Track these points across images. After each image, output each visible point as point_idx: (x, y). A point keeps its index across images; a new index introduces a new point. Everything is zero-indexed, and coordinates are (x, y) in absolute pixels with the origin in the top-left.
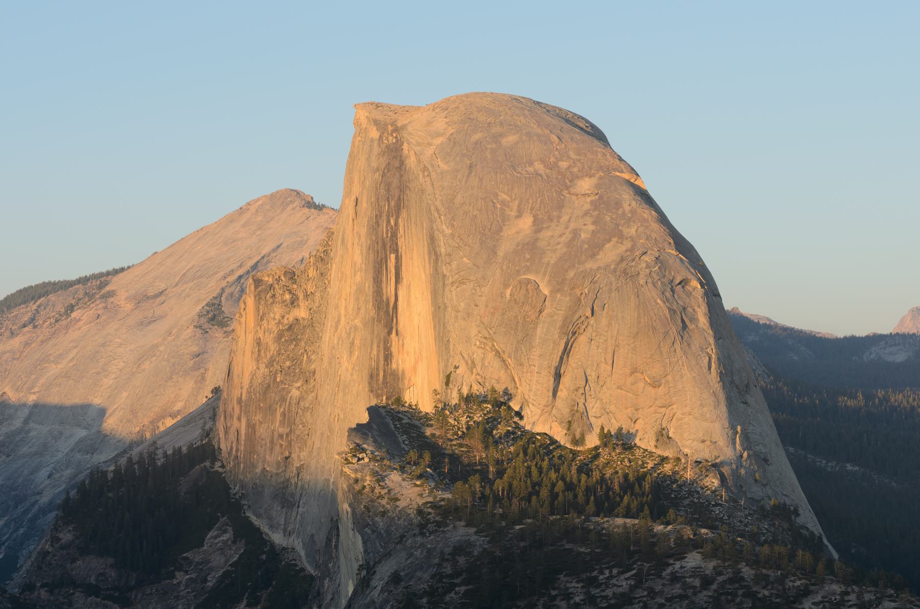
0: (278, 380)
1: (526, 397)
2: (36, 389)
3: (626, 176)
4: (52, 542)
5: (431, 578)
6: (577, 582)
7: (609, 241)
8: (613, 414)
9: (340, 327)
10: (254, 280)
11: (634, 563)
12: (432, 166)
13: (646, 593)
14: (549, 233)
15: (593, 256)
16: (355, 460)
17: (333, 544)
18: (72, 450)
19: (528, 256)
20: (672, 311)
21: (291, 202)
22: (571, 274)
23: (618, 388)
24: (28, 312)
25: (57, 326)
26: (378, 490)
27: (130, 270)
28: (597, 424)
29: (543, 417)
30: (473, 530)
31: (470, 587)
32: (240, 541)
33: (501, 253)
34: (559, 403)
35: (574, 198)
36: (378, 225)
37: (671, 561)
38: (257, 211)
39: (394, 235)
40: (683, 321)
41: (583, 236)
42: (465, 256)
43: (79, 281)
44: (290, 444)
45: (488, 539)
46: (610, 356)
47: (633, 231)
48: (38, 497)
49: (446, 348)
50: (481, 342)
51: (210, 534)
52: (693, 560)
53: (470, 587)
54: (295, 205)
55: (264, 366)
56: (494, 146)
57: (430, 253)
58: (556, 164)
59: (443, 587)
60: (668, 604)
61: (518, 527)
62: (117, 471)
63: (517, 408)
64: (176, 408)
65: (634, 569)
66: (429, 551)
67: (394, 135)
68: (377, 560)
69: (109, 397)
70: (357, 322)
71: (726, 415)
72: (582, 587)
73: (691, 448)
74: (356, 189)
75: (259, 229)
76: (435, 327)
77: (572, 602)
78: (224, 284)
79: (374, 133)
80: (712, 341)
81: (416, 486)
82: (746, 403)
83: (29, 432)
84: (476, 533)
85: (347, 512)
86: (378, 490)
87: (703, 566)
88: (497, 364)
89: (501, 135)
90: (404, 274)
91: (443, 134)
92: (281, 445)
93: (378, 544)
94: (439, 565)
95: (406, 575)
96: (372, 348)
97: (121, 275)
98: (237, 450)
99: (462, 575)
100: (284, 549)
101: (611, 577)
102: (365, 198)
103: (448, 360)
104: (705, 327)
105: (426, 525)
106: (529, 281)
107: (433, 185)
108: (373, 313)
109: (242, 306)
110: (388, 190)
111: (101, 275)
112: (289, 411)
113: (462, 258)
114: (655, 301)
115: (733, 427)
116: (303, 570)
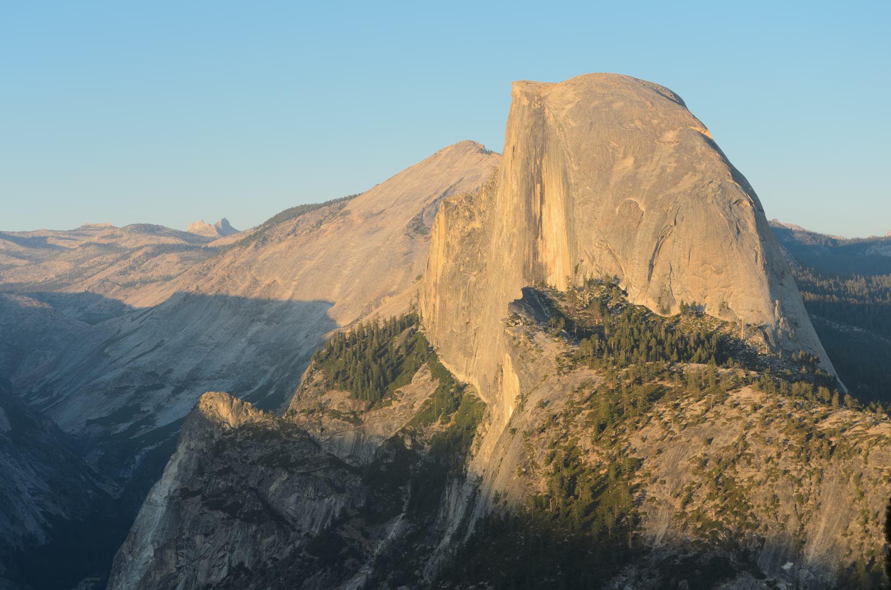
0: (461, 270)
1: (630, 281)
2: (297, 278)
3: (698, 129)
5: (567, 403)
6: (667, 407)
7: (686, 174)
10: (444, 203)
13: (713, 415)
14: (645, 169)
15: (676, 184)
16: (513, 324)
17: (499, 381)
18: (322, 319)
19: (630, 185)
20: (730, 222)
22: (660, 197)
23: (693, 274)
24: (290, 225)
25: (311, 234)
26: (529, 344)
28: (678, 299)
29: (641, 295)
31: (592, 410)
33: (612, 183)
34: (653, 285)
35: (662, 144)
36: (529, 164)
38: (446, 156)
39: (539, 171)
40: (738, 229)
41: (668, 170)
42: (587, 185)
43: (326, 204)
45: (604, 377)
46: (687, 252)
47: (702, 167)
49: (575, 248)
50: (599, 244)
51: (417, 374)
52: (745, 392)
53: (592, 410)
55: (451, 260)
56: (607, 110)
57: (563, 183)
58: (650, 121)
60: (728, 423)
62: (352, 333)
63: (623, 289)
64: (392, 290)
66: (564, 386)
67: (539, 103)
69: (347, 283)
70: (515, 231)
71: (768, 293)
72: (670, 411)
74: (513, 141)
75: (449, 167)
76: (567, 233)
78: (424, 205)
79: (525, 102)
80: (758, 242)
82: (782, 285)
84: (596, 373)
85: (508, 360)
86: (529, 344)
88: (610, 258)
89: (612, 102)
90: (546, 198)
91: (572, 102)
92: (464, 315)
93: (529, 381)
94: (571, 396)
96: (524, 248)
97: (354, 200)
98: (434, 318)
100: (466, 385)
101: (689, 404)
103: (576, 256)
104: (753, 233)
106: (631, 202)
107: (565, 136)
108: (525, 224)
109: (436, 220)
110: (535, 141)
111: (341, 200)
112: (469, 291)
113: (586, 186)
114: (719, 215)
115: (773, 301)
116: (479, 399)
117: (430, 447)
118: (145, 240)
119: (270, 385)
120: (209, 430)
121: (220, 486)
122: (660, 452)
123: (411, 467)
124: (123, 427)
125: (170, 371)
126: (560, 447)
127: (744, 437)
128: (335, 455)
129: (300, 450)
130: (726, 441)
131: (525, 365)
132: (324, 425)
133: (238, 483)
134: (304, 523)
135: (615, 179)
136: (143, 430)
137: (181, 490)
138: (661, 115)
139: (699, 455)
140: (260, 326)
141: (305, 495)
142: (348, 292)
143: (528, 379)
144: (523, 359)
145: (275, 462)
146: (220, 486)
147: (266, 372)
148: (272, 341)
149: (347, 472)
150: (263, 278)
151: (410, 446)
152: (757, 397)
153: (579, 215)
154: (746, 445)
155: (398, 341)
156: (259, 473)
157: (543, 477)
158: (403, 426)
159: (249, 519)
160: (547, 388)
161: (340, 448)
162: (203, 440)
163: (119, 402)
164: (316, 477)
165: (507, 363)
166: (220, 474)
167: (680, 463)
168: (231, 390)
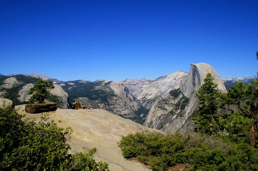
47: (214, 73)
118: (144, 80)
119: (159, 95)
124: (144, 99)
134: (169, 110)
136: (146, 99)
155: (178, 91)
159: (163, 109)
163: (143, 97)
166: (160, 104)
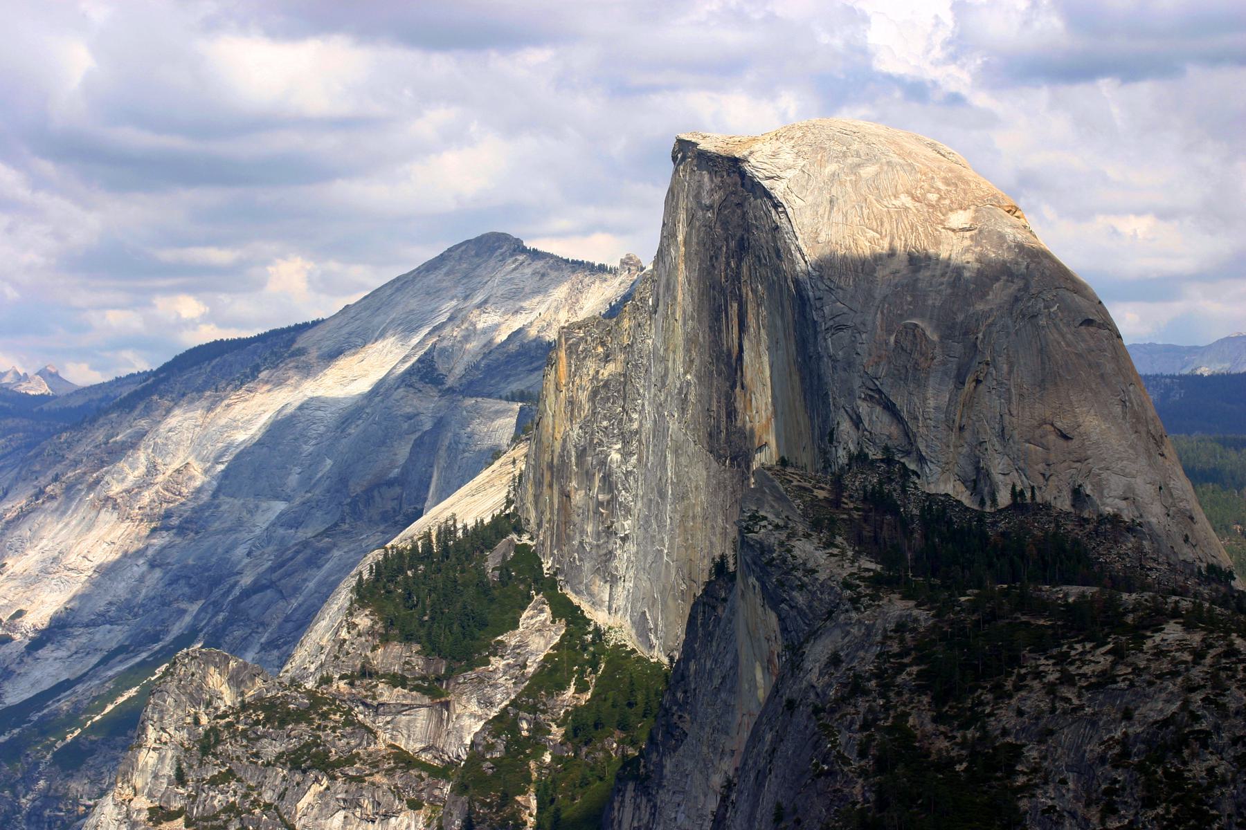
1: (924, 454)
2: (225, 459)
4: (348, 629)
5: (878, 657)
6: (1046, 659)
7: (998, 279)
8: (1022, 470)
9: (668, 382)
11: (1108, 635)
12: (787, 200)
13: (1130, 670)
14: (928, 273)
15: (983, 296)
18: (273, 524)
19: (909, 299)
21: (500, 247)
27: (320, 326)
30: (911, 603)
31: (923, 667)
32: (560, 621)
35: (951, 233)
37: (1149, 634)
39: (737, 276)
43: (260, 338)
44: (612, 513)
45: (932, 613)
48: (238, 577)
49: (824, 402)
52: (1173, 632)
53: (923, 667)
54: (503, 250)
55: (578, 426)
56: (853, 178)
58: (924, 195)
59: (892, 668)
60: (1158, 682)
61: (963, 599)
65: (1109, 643)
66: (869, 629)
68: (802, 640)
69: (310, 465)
72: (1054, 664)
73: (1111, 506)
76: (802, 380)
77: (1046, 680)
81: (832, 555)
82: (1162, 455)
83: (218, 506)
85: (754, 587)
87: (1188, 637)
88: (886, 418)
89: (859, 165)
94: (883, 644)
95: (847, 655)
97: (315, 328)
99: (910, 654)
102: (695, 240)
105: (860, 596)
106: (916, 325)
111: (283, 331)
114: (1059, 343)
117: (562, 731)
120: (193, 711)
121: (216, 802)
122: (1051, 733)
123: (532, 764)
125: (20, 614)
126: (879, 729)
127: (1186, 703)
128: (402, 747)
129: (344, 741)
130: (1161, 711)
131: (789, 595)
132: (381, 700)
133: (246, 796)
135: (878, 293)
137: (149, 809)
138: (943, 187)
139: (1118, 735)
140: (167, 539)
141: (358, 814)
142: (313, 481)
143: (798, 618)
144: (783, 586)
145: (305, 761)
146: (216, 802)
147: (183, 612)
148: (191, 562)
149: (424, 774)
150: (168, 460)
151: (527, 730)
152: (1196, 638)
153: (827, 348)
154: (1196, 718)
155: (492, 562)
156: (279, 779)
157: (860, 777)
158: (513, 697)
160: (837, 633)
161: (409, 736)
162: (183, 728)
164: (373, 784)
165: (751, 594)
166: (214, 782)
167: (1089, 748)
168: (127, 643)
